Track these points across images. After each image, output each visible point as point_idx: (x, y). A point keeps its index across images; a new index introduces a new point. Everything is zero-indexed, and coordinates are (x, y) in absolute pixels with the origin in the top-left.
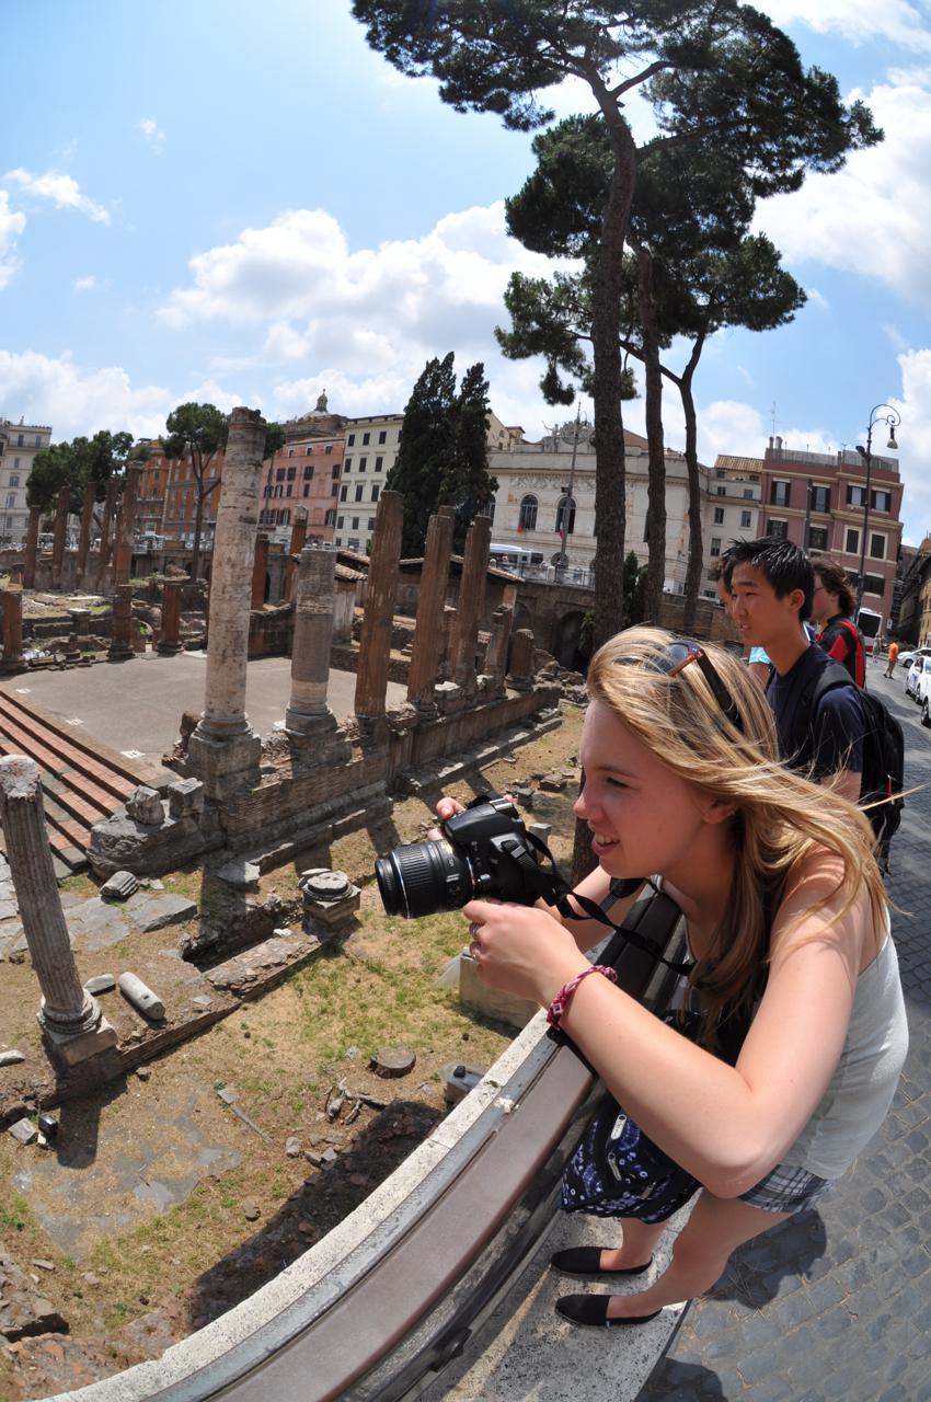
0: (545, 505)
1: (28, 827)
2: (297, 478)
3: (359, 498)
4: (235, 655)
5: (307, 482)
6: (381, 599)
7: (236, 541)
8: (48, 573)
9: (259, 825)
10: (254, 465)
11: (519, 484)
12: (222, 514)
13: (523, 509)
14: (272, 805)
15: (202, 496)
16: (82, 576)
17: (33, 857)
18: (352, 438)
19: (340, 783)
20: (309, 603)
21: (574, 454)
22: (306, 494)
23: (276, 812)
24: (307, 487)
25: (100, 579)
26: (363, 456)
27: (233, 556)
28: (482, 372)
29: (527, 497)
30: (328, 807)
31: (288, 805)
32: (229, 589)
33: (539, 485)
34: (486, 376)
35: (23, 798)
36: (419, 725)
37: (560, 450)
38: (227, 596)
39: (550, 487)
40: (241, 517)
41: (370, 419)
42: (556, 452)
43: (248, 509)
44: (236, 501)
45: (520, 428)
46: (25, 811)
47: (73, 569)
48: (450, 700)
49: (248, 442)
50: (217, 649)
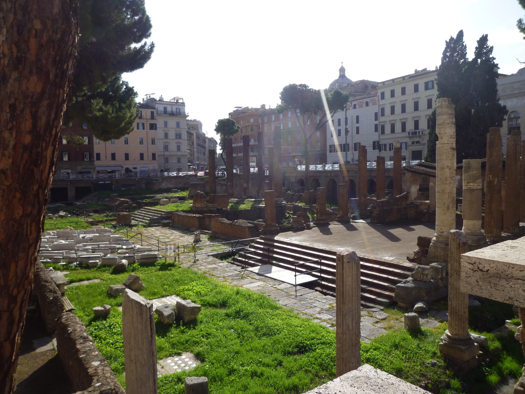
3: (393, 131)
7: (450, 158)
8: (224, 187)
18: (383, 94)
20: (471, 184)
22: (358, 132)
26: (392, 105)
27: (449, 165)
28: (487, 40)
34: (490, 43)
38: (448, 182)
44: (448, 140)
50: (444, 205)
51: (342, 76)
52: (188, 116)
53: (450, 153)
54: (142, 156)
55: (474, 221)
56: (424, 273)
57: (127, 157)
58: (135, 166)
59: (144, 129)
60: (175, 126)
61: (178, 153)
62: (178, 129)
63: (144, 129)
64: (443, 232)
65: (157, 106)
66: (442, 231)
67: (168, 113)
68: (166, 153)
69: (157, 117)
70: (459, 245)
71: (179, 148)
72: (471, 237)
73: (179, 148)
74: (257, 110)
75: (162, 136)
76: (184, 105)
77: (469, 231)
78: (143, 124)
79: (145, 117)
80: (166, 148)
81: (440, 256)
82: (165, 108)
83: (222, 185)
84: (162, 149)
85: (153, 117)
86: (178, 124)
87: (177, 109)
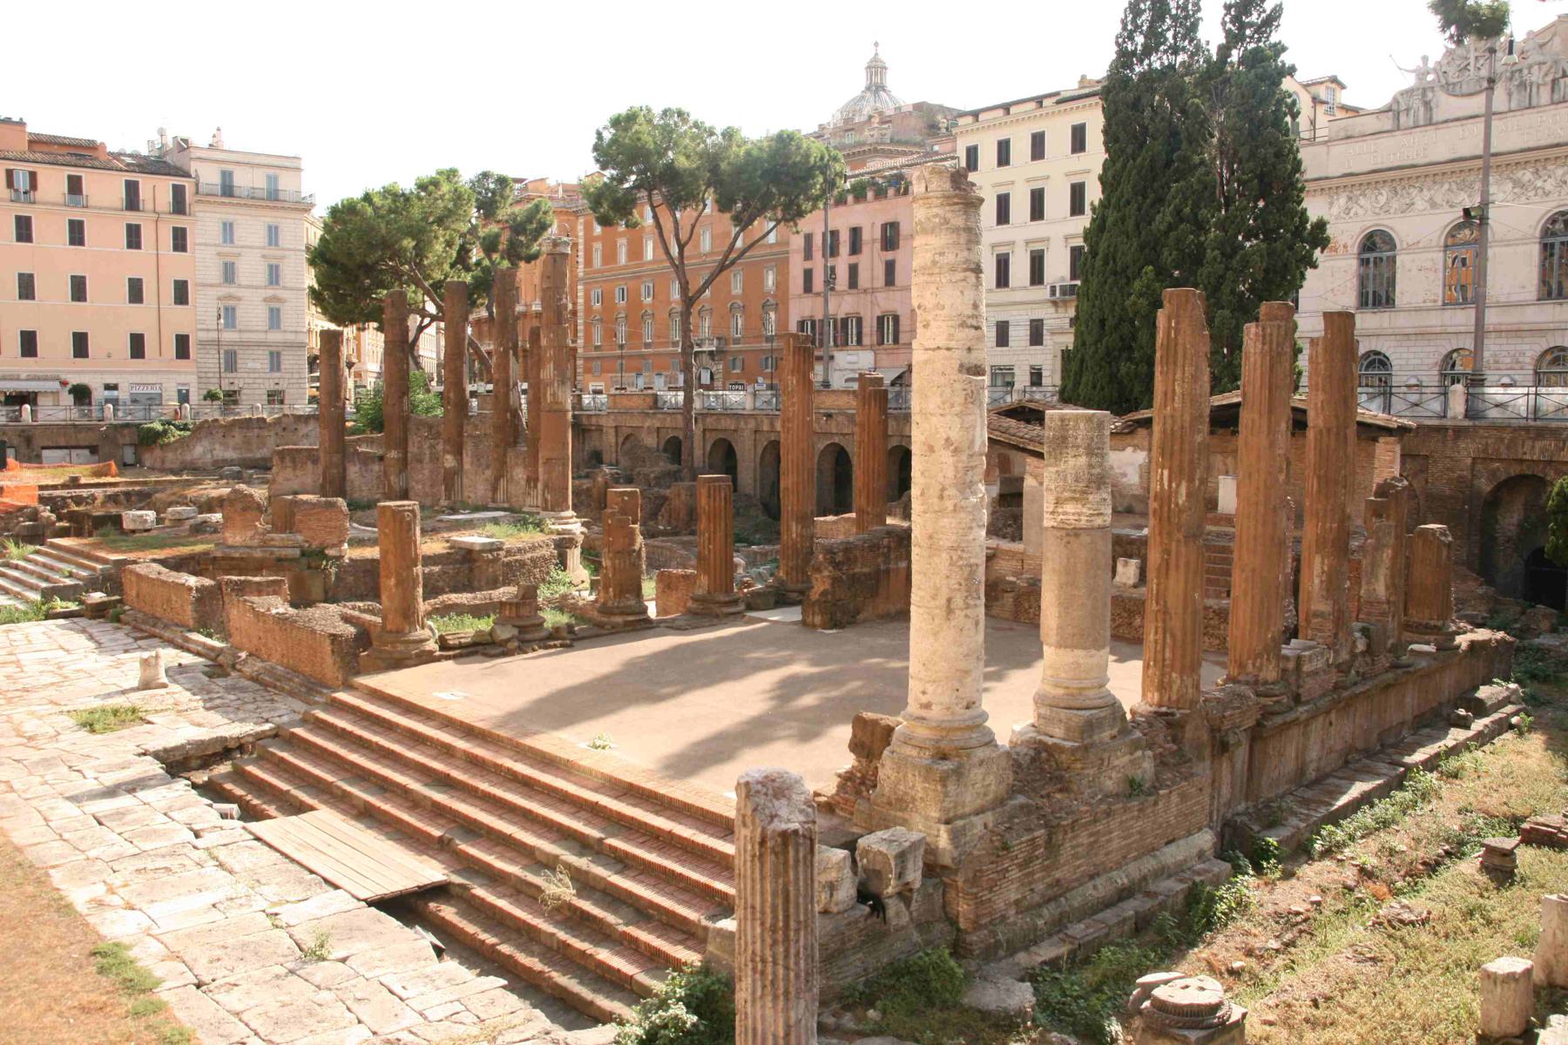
0: (1413, 248)
1: (797, 879)
2: (866, 249)
4: (968, 606)
5: (889, 255)
6: (1183, 490)
8: (376, 467)
9: (1012, 912)
10: (972, 270)
11: (1348, 210)
12: (926, 362)
13: (1364, 262)
14: (1033, 873)
15: (689, 301)
17: (797, 931)
19: (1139, 832)
20: (1070, 508)
21: (1489, 115)
23: (1040, 887)
24: (890, 267)
25: (497, 479)
27: (955, 435)
29: (1370, 236)
30: (1122, 879)
31: (1058, 874)
32: (951, 491)
33: (1395, 205)
35: (796, 832)
36: (1259, 724)
37: (1438, 116)
38: (949, 504)
39: (1420, 204)
40: (961, 366)
41: (1006, 108)
42: (1430, 123)
43: (969, 349)
45: (1334, 80)
46: (797, 852)
47: (435, 459)
48: (1309, 674)
49: (957, 230)
50: (934, 598)
51: (876, 87)
52: (312, 205)
53: (958, 386)
54: (137, 346)
55: (1080, 652)
57: (81, 345)
58: (111, 380)
61: (275, 337)
62: (273, 252)
64: (927, 706)
65: (194, 167)
66: (924, 699)
68: (229, 336)
69: (196, 208)
70: (763, 843)
71: (275, 318)
72: (1063, 714)
73: (275, 318)
75: (214, 274)
77: (1061, 691)
79: (149, 206)
82: (227, 177)
83: (366, 459)
85: (179, 206)
86: (273, 234)
87: (269, 177)
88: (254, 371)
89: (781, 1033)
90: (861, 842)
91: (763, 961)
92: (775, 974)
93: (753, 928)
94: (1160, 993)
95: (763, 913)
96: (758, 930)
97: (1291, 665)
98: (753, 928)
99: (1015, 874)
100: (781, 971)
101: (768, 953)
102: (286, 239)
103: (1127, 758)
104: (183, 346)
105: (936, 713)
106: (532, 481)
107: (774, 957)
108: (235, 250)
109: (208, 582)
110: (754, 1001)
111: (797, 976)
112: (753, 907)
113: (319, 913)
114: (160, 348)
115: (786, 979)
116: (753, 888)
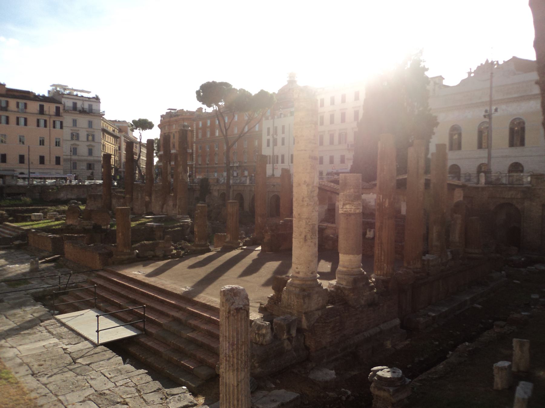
1: (241, 326)
4: (312, 238)
6: (387, 201)
8: (122, 200)
16: (150, 202)
20: (348, 206)
25: (163, 204)
32: (307, 199)
38: (305, 203)
43: (312, 151)
50: (300, 235)
54: (42, 160)
56: (260, 332)
59: (45, 126)
60: (86, 125)
62: (90, 130)
63: (45, 126)
64: (298, 273)
65: (63, 100)
66: (297, 270)
67: (78, 109)
68: (74, 157)
69: (63, 114)
70: (229, 312)
71: (90, 152)
72: (346, 277)
73: (90, 152)
74: (192, 113)
76: (100, 102)
78: (45, 121)
79: (47, 113)
80: (74, 151)
81: (294, 305)
82: (75, 104)
84: (68, 153)
85: (58, 113)
86: (90, 124)
88: (83, 169)
89: (236, 385)
90: (275, 320)
91: (229, 356)
92: (233, 362)
93: (226, 344)
94: (379, 373)
95: (229, 338)
96: (228, 345)
97: (426, 263)
98: (226, 344)
99: (329, 332)
100: (235, 360)
101: (231, 353)
102: (94, 126)
103: (368, 293)
104: (58, 161)
105: (301, 275)
106: (175, 205)
107: (233, 355)
108: (77, 129)
109: (58, 236)
110: (226, 372)
111: (241, 362)
112: (226, 336)
113: (82, 348)
114: (50, 161)
115: (237, 363)
116: (226, 329)
